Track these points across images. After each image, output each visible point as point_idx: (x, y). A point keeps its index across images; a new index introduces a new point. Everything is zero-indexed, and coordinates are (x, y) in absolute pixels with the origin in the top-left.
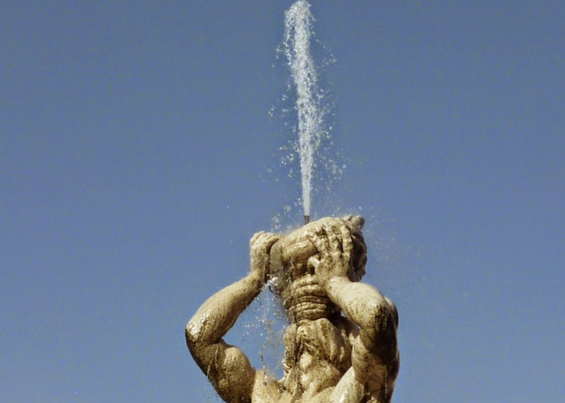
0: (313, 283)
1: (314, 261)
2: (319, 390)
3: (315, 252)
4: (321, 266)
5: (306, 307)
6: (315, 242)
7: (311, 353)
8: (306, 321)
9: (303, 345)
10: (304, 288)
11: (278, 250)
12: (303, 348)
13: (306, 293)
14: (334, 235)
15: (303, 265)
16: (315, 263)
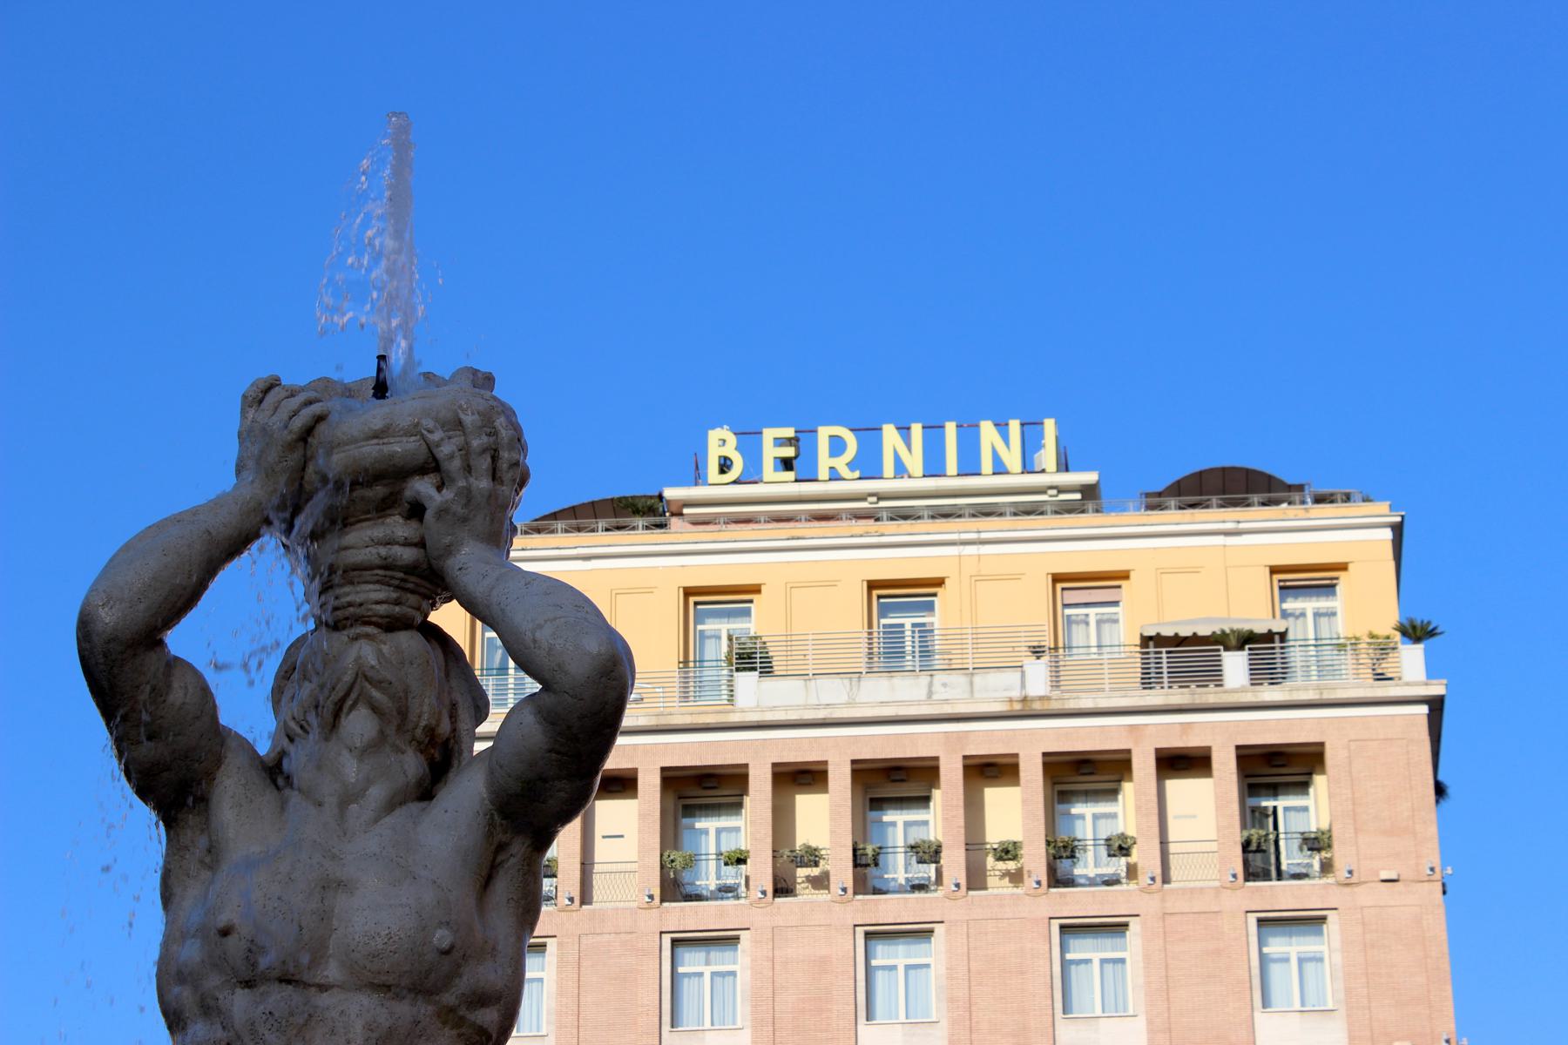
0: (406, 543)
1: (422, 487)
2: (391, 805)
3: (430, 465)
4: (442, 512)
5: (381, 596)
6: (438, 446)
7: (375, 709)
8: (370, 630)
9: (362, 688)
10: (383, 551)
11: (1257, 826)
12: (359, 695)
13: (387, 566)
14: (485, 439)
15: (391, 494)
16: (431, 498)
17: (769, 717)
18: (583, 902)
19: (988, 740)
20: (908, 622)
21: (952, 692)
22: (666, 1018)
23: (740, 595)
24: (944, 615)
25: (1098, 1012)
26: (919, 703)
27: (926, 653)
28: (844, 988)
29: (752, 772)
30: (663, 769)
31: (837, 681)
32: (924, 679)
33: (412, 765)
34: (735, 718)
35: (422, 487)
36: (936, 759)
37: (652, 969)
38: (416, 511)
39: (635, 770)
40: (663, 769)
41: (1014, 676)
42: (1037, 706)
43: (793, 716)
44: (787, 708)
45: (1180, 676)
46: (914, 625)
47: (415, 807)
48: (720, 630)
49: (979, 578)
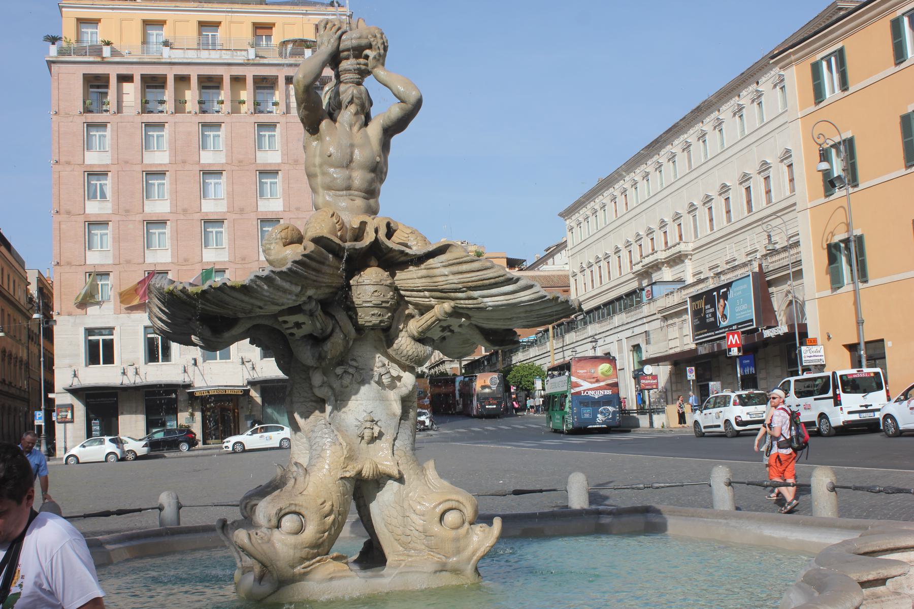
2: (360, 128)
3: (370, 47)
17: (173, 61)
18: (118, 113)
19: (237, 71)
20: (210, 34)
21: (226, 57)
22: (144, 147)
23: (161, 23)
24: (220, 33)
25: (268, 149)
26: (217, 59)
27: (214, 44)
28: (195, 140)
29: (168, 77)
30: (141, 75)
31: (193, 51)
32: (219, 52)
33: (363, 117)
34: (163, 61)
35: (367, 52)
36: (222, 75)
37: (138, 134)
38: (367, 57)
39: (133, 75)
40: (141, 75)
41: (244, 53)
42: (251, 62)
43: (180, 61)
44: (179, 58)
45: (293, 54)
46: (212, 35)
47: (364, 129)
48: (153, 33)
49: (231, 22)
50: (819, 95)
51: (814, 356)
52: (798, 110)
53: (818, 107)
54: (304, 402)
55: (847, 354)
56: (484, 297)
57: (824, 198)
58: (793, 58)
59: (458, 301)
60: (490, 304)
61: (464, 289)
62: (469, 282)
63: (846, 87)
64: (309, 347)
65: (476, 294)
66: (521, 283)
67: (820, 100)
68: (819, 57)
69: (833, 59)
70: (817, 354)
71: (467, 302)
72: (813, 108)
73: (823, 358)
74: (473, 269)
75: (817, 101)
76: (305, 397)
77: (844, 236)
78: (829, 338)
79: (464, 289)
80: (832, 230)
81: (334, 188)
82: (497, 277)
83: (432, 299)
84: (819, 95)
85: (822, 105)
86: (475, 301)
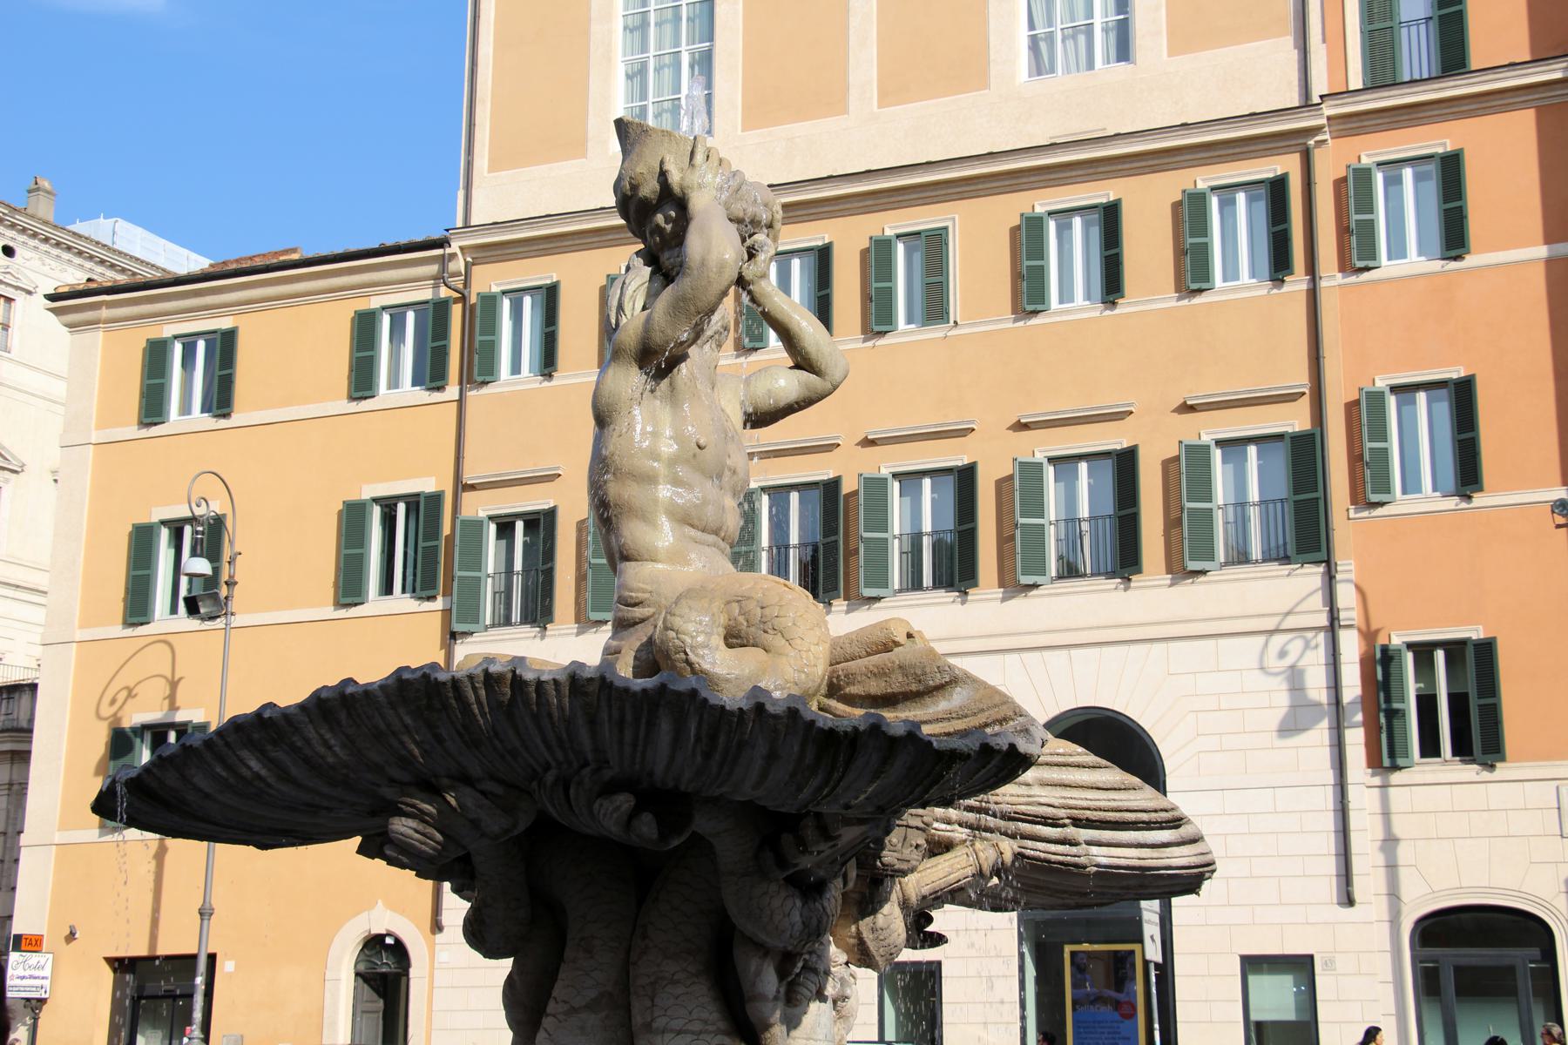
50: (152, 408)
51: (31, 977)
52: (93, 426)
53: (145, 433)
54: (701, 1032)
55: (108, 975)
56: (1089, 843)
57: (121, 627)
58: (105, 313)
59: (1029, 843)
60: (1104, 861)
61: (1067, 821)
62: (1089, 809)
63: (225, 411)
64: (799, 903)
65: (1085, 834)
66: (1184, 832)
67: (156, 420)
68: (168, 331)
69: (201, 345)
70: (36, 973)
71: (1060, 848)
72: (133, 431)
73: (47, 983)
74: (1101, 785)
75: (149, 420)
76: (705, 1022)
77: (153, 716)
78: (71, 936)
79: (1067, 821)
80: (130, 701)
81: (696, 522)
82: (1156, 811)
83: (956, 827)
84: (152, 408)
85: (155, 431)
86: (1074, 850)
